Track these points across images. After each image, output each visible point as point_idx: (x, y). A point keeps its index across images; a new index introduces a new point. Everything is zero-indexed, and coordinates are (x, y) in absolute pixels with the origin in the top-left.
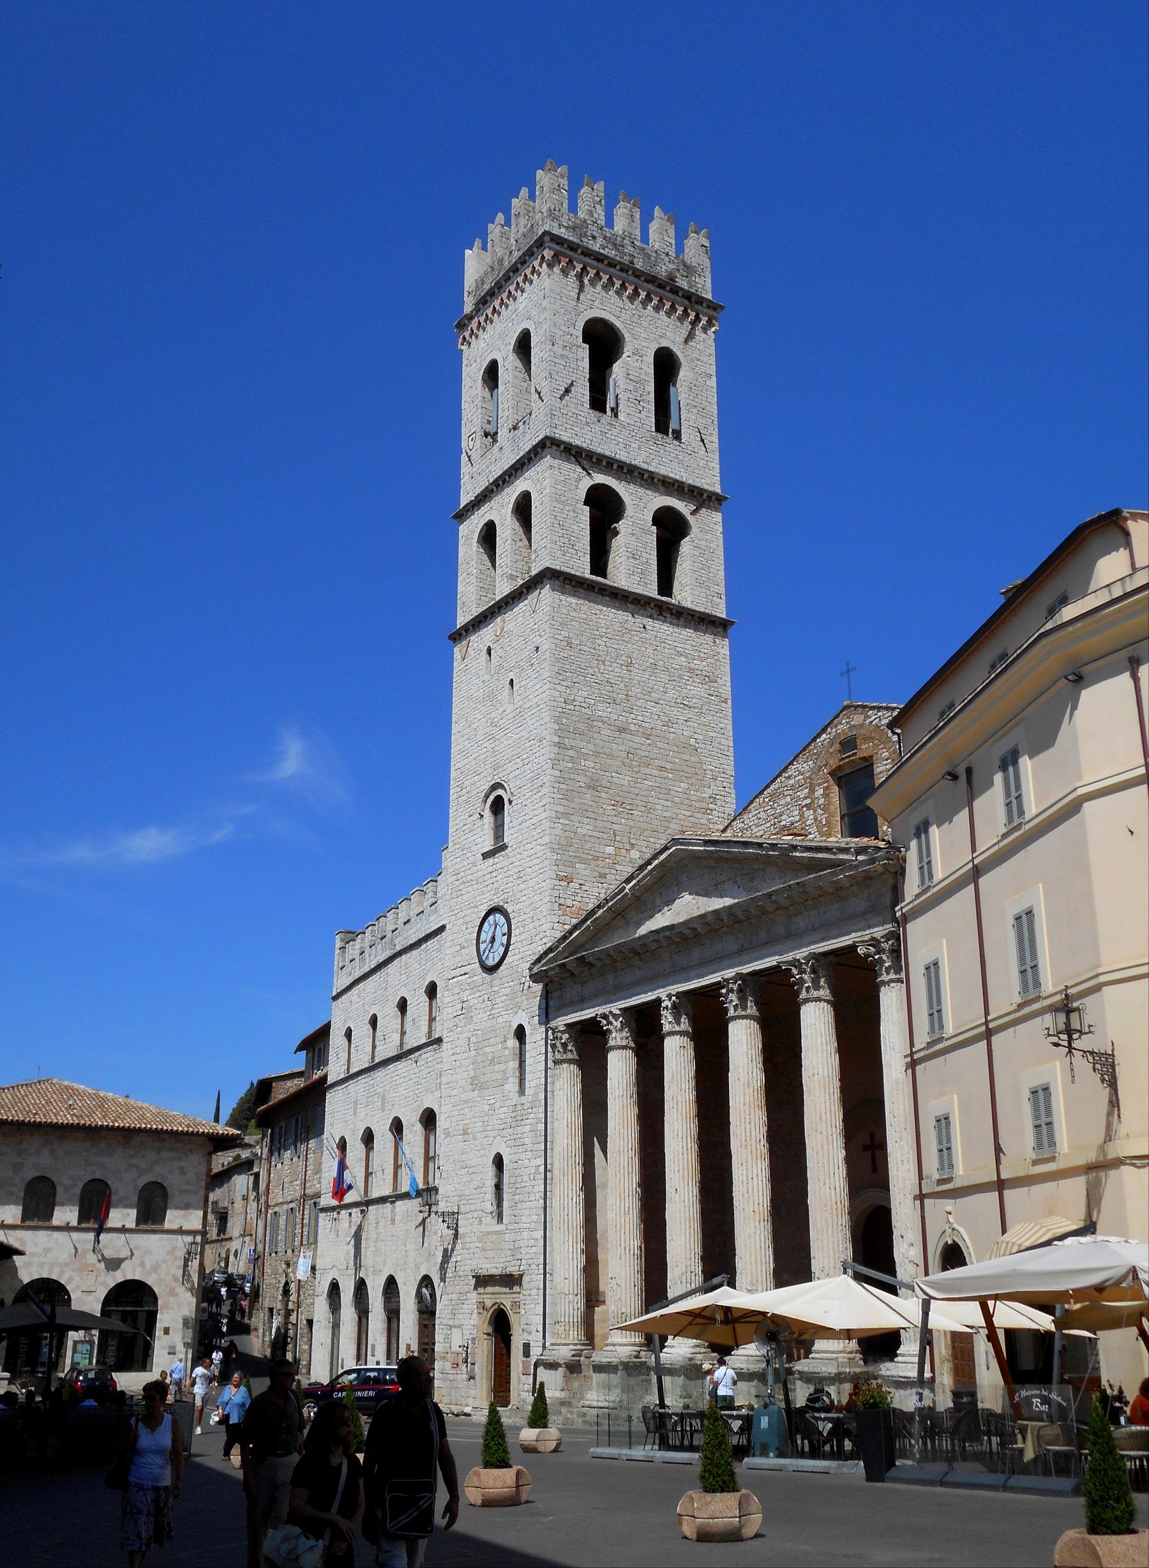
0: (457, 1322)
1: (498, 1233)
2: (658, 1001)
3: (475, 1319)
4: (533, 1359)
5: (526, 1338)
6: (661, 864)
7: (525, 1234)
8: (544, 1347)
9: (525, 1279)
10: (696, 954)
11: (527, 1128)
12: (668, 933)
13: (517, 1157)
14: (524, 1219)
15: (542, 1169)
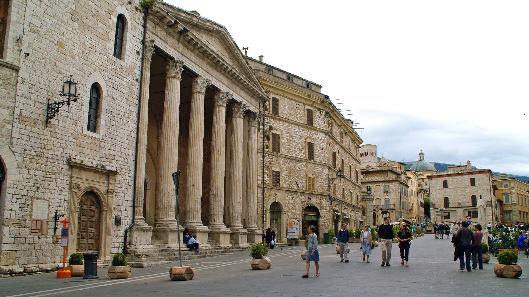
0: (41, 195)
1: (95, 139)
2: (197, 76)
3: (66, 195)
4: (123, 228)
5: (115, 214)
6: (218, 30)
7: (118, 148)
8: (133, 221)
9: (118, 177)
10: (215, 73)
11: (124, 83)
12: (221, 60)
13: (115, 96)
14: (118, 139)
15: (135, 114)
